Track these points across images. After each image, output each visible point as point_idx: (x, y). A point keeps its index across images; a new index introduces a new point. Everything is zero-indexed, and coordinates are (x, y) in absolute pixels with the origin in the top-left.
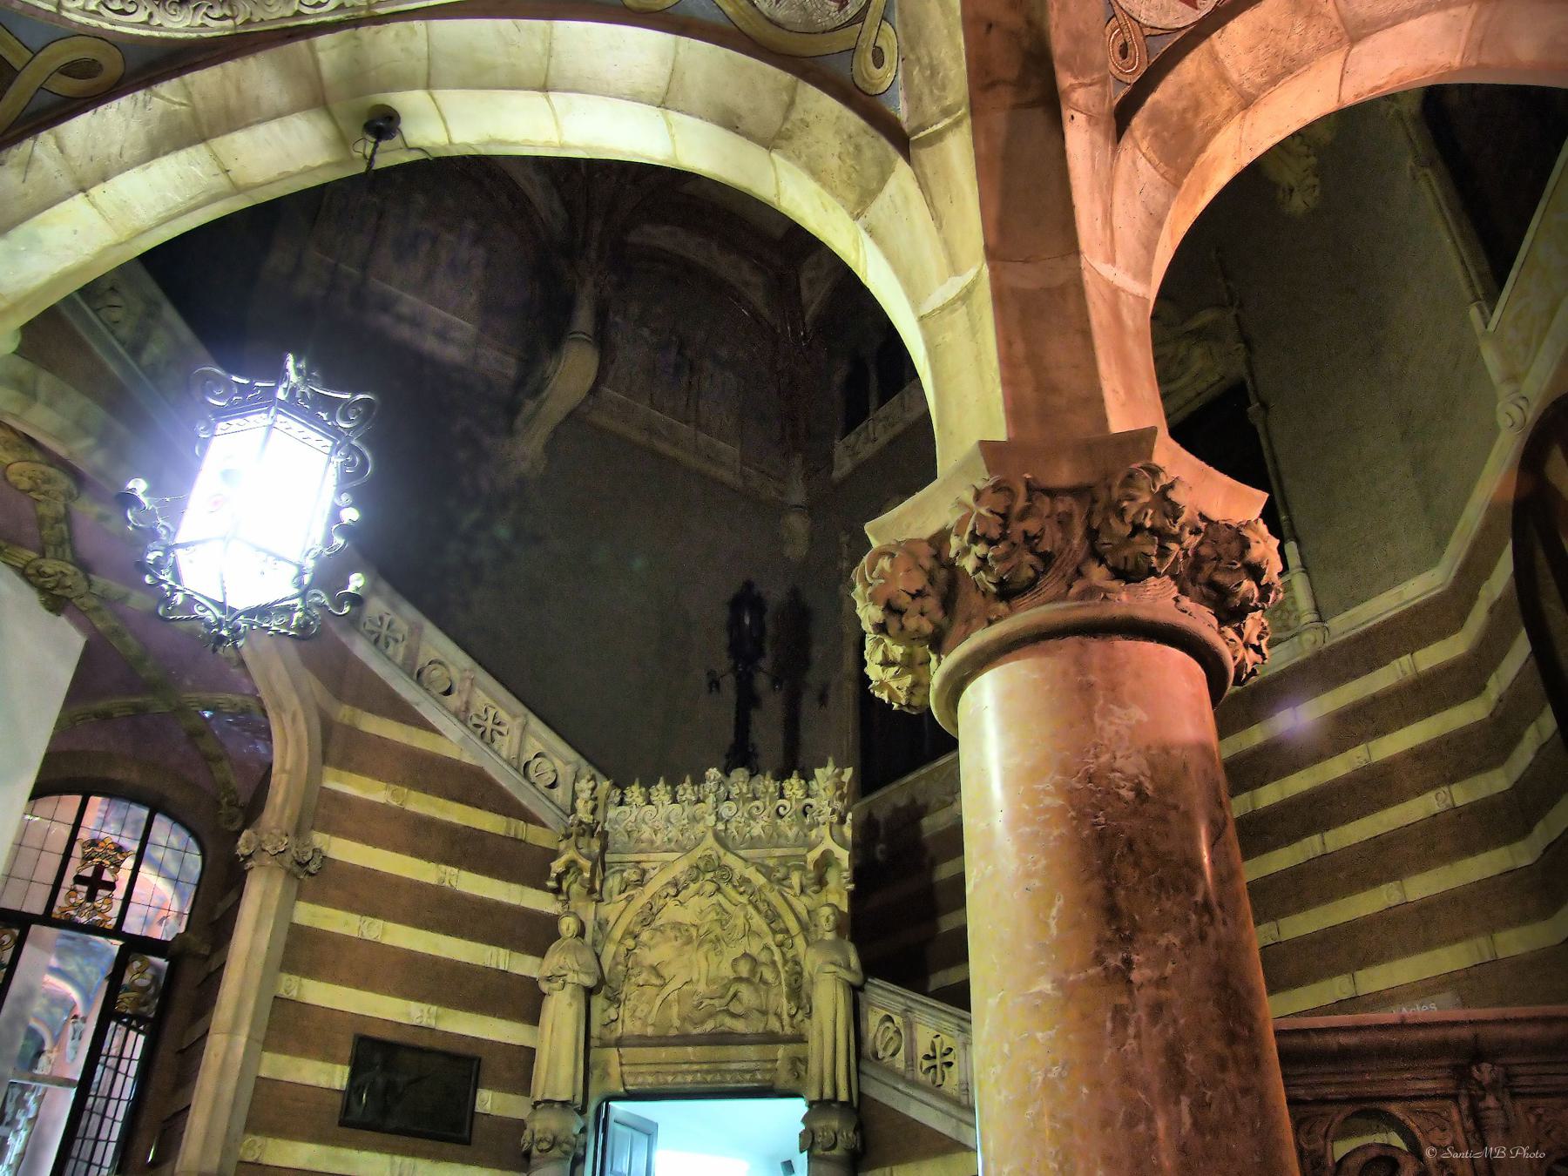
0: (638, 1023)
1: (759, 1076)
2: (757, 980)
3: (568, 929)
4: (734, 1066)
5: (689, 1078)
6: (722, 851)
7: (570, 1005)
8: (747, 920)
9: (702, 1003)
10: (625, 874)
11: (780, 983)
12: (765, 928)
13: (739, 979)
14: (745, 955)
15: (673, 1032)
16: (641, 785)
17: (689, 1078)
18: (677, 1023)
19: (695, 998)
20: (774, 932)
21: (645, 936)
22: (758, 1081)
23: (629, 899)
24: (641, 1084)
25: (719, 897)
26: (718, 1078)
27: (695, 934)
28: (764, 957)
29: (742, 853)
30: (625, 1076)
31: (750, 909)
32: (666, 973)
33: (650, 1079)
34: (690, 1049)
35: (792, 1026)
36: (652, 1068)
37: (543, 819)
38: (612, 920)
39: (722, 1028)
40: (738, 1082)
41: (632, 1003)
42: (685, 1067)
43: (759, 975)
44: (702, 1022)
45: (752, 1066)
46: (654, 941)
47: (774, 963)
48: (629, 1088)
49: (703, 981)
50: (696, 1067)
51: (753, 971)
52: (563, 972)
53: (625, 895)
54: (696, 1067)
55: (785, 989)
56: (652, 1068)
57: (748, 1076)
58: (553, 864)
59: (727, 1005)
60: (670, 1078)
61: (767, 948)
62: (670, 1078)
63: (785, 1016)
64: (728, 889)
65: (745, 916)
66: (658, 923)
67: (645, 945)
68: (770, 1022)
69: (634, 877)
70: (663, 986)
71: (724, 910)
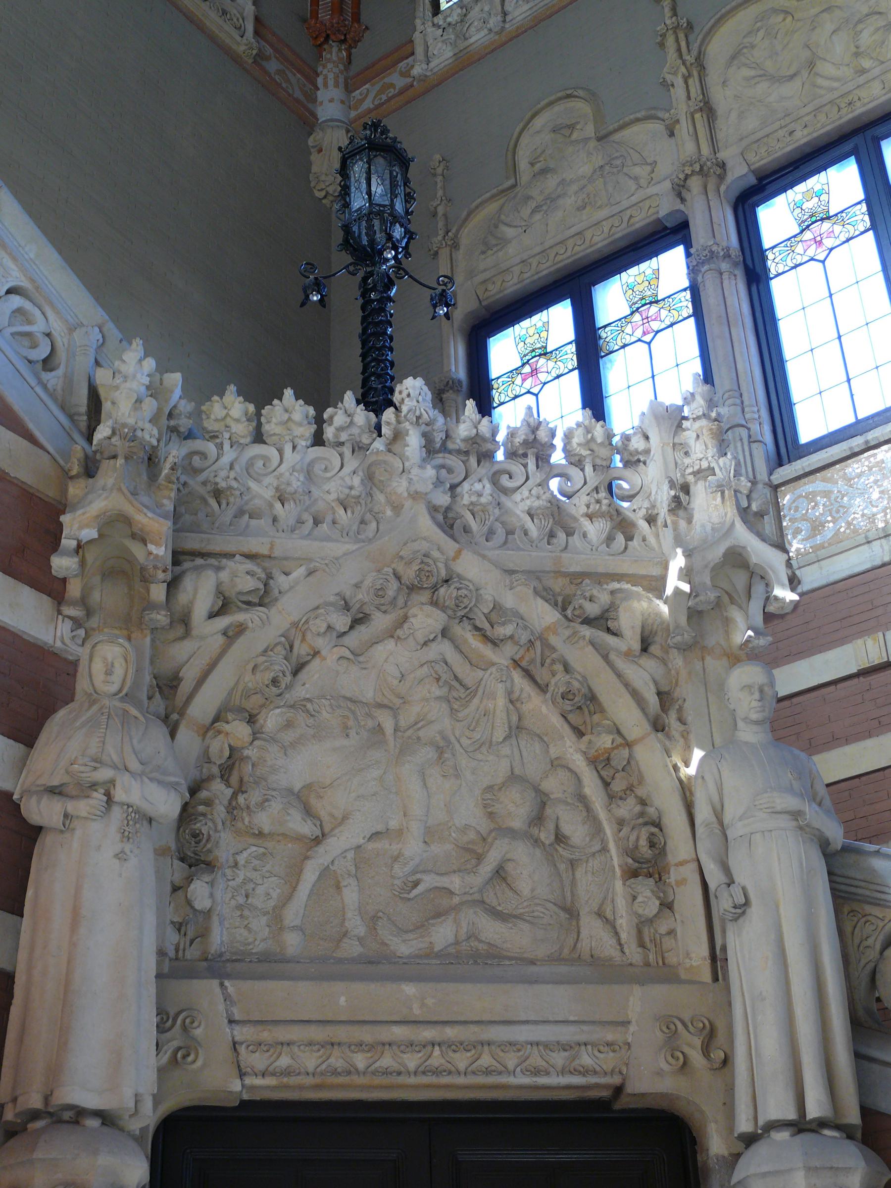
0: (259, 924)
1: (586, 1059)
2: (546, 836)
3: (109, 672)
4: (522, 1034)
5: (412, 1061)
6: (451, 546)
7: (120, 856)
8: (511, 702)
9: (416, 884)
10: (224, 575)
11: (604, 849)
12: (556, 720)
13: (512, 833)
14: (513, 778)
15: (351, 948)
16: (246, 394)
17: (412, 1061)
18: (356, 925)
19: (398, 870)
20: (579, 733)
21: (271, 720)
22: (585, 1072)
23: (232, 635)
24: (287, 1072)
25: (445, 648)
26: (486, 1060)
27: (388, 725)
28: (554, 785)
29: (493, 554)
30: (242, 1050)
31: (517, 678)
32: (321, 808)
33: (310, 1061)
34: (409, 989)
35: (642, 945)
36: (317, 1034)
37: (31, 426)
38: (189, 675)
39: (474, 944)
40: (537, 1072)
41: (241, 875)
42: (399, 1032)
43: (552, 827)
44: (421, 927)
45: (566, 1034)
46: (288, 737)
47: (582, 798)
48: (248, 1081)
49: (416, 829)
50: (428, 1034)
51: (538, 819)
52: (105, 774)
53: (223, 622)
54: (428, 1034)
55: (616, 859)
56: (317, 1034)
57: (559, 1058)
58: (63, 518)
59: (480, 891)
60: (360, 1060)
61: (557, 764)
62: (360, 1060)
63: (624, 923)
64: (464, 633)
65: (509, 693)
66: (300, 692)
67: (273, 740)
68: (584, 933)
69: (248, 584)
70: (317, 841)
71: (456, 678)
